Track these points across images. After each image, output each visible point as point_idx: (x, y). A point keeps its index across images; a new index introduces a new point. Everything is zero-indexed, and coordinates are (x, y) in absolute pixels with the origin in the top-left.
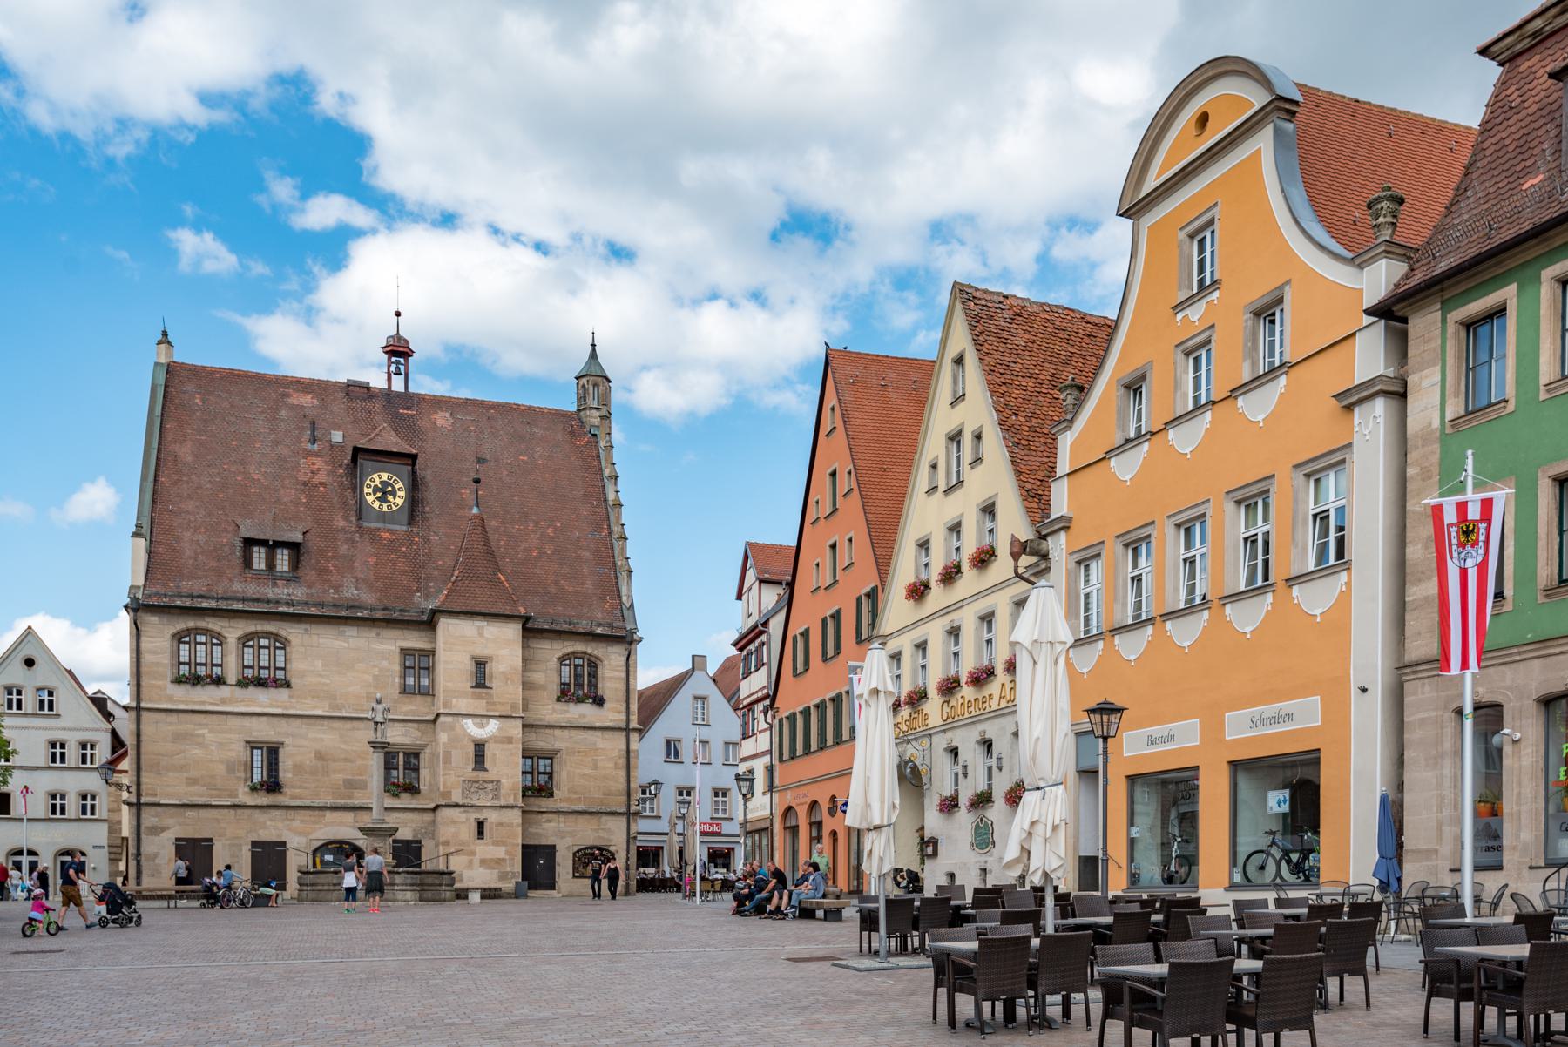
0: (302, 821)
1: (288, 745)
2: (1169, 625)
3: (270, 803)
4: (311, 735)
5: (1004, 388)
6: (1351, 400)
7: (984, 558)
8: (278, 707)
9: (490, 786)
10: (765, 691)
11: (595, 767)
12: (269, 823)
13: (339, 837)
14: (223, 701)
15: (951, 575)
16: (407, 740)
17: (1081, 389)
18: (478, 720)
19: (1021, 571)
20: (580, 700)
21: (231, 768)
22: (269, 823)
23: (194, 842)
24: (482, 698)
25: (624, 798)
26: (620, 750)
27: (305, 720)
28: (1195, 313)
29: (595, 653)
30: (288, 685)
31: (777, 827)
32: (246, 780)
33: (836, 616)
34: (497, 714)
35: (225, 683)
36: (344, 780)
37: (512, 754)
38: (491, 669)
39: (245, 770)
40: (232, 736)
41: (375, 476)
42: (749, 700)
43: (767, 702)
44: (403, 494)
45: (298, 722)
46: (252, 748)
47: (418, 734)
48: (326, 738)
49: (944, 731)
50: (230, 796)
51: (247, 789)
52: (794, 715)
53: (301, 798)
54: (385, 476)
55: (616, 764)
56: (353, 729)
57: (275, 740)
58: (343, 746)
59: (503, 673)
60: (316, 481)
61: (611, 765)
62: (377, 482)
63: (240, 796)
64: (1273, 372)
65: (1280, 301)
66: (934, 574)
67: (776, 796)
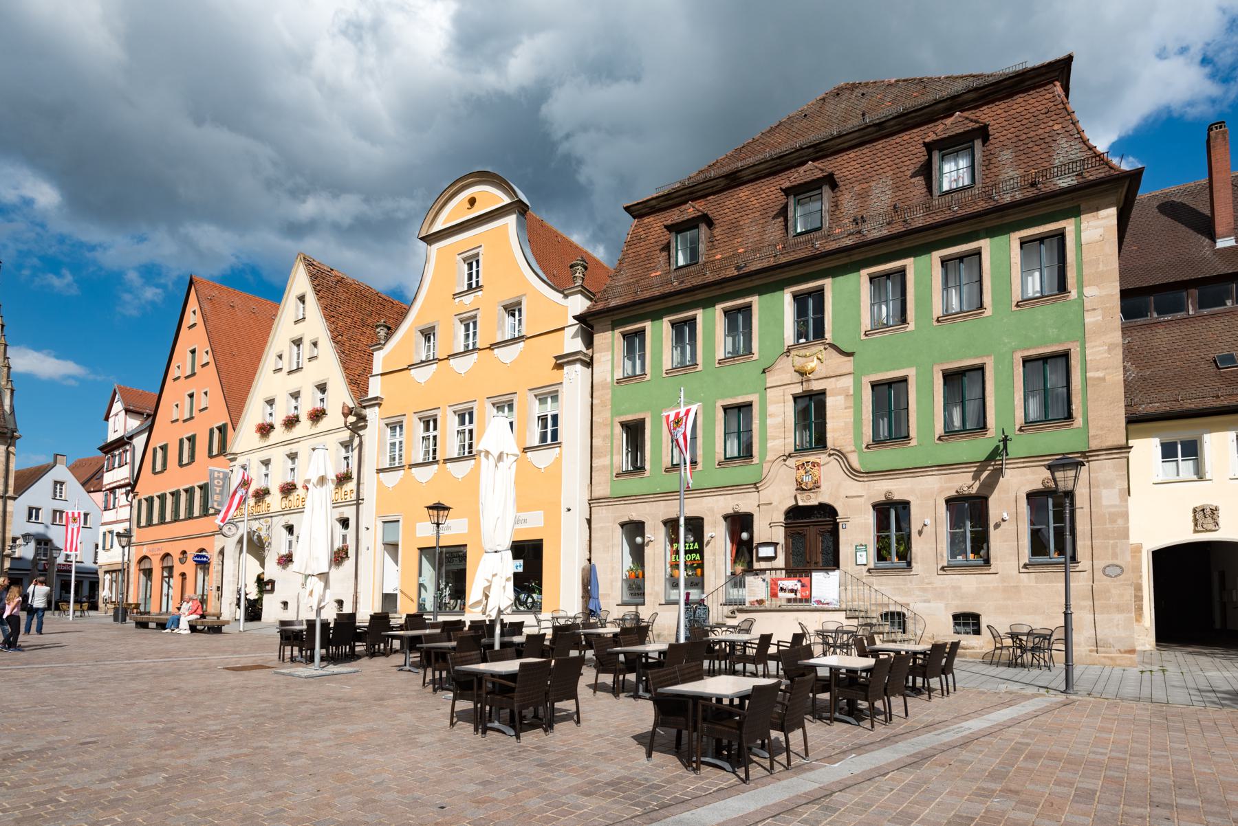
2: (449, 465)
5: (333, 319)
6: (561, 362)
7: (317, 416)
10: (127, 481)
15: (291, 422)
17: (389, 328)
19: (348, 424)
28: (468, 299)
31: (133, 568)
33: (192, 439)
42: (112, 486)
43: (129, 488)
49: (283, 515)
52: (152, 498)
64: (521, 338)
65: (520, 303)
66: (278, 421)
67: (133, 549)
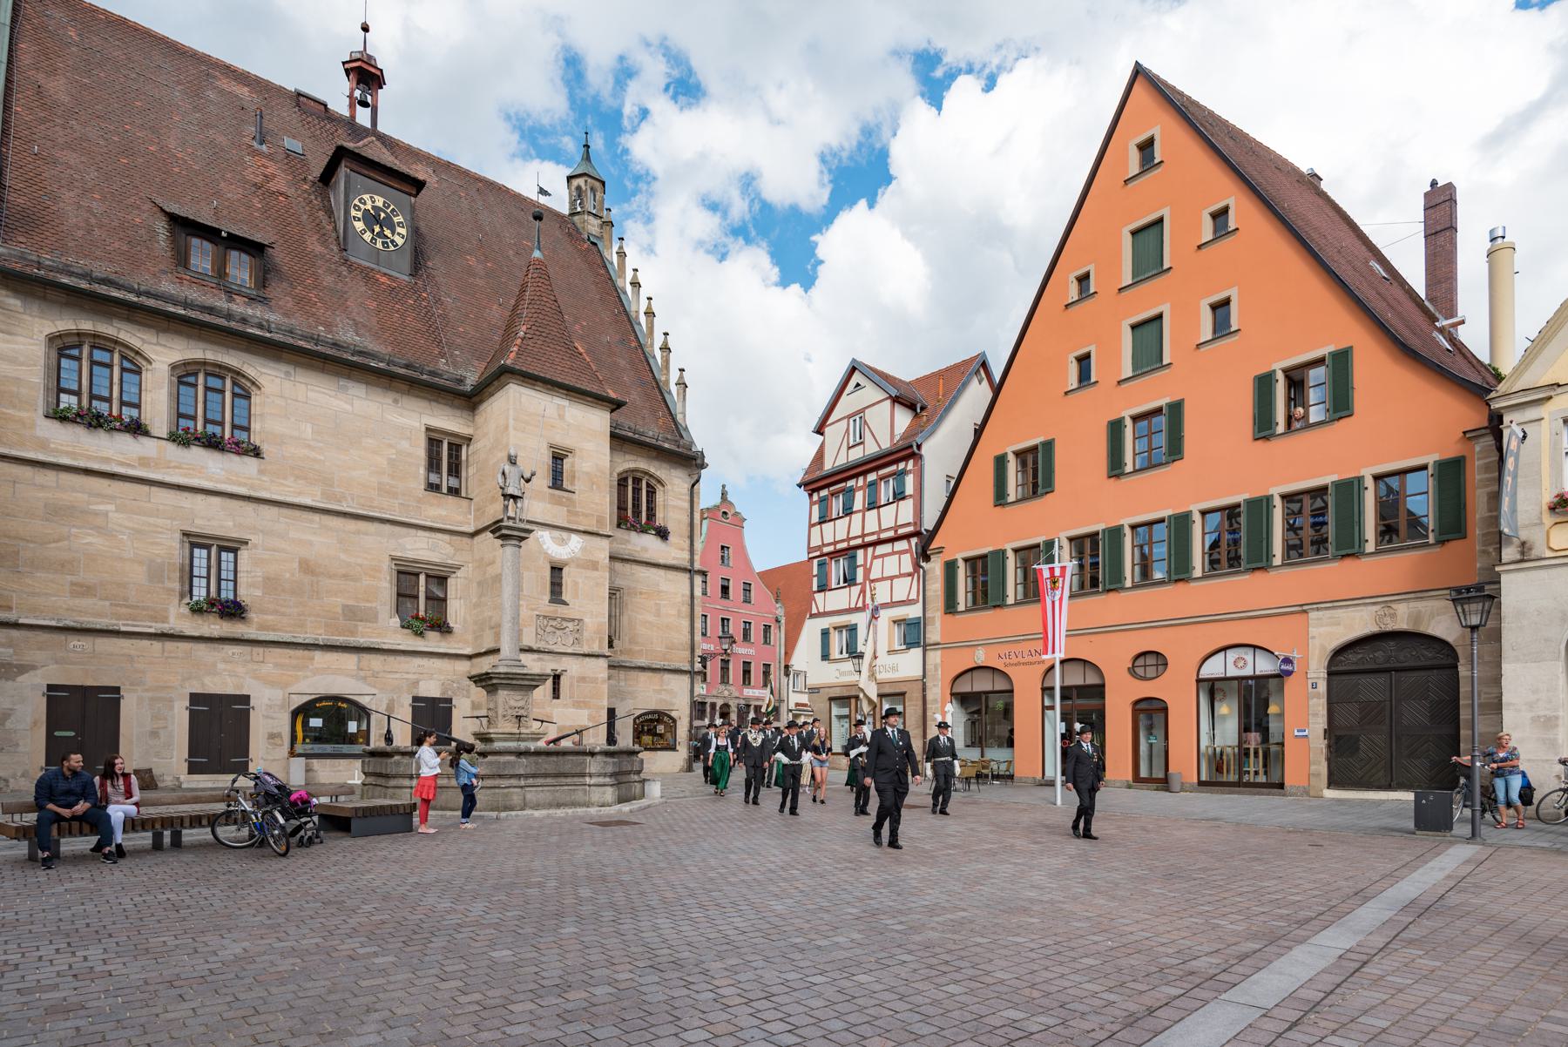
0: (276, 665)
1: (255, 546)
3: (224, 634)
4: (292, 534)
8: (240, 484)
9: (570, 625)
11: (658, 614)
12: (221, 666)
13: (335, 690)
14: (144, 462)
16: (434, 557)
18: (557, 533)
20: (644, 531)
21: (156, 573)
22: (221, 666)
23: (84, 694)
24: (560, 504)
25: (688, 653)
26: (683, 595)
27: (285, 511)
29: (658, 473)
30: (256, 453)
32: (182, 596)
34: (581, 528)
35: (146, 433)
36: (345, 607)
37: (597, 584)
38: (573, 465)
39: (181, 578)
40: (160, 521)
41: (367, 197)
44: (403, 231)
45: (275, 510)
46: (193, 545)
47: (449, 550)
48: (319, 539)
50: (154, 619)
51: (185, 610)
53: (274, 630)
54: (380, 202)
55: (679, 611)
56: (358, 532)
57: (235, 535)
58: (343, 556)
59: (587, 473)
60: (273, 186)
61: (674, 612)
62: (369, 207)
63: (172, 620)
